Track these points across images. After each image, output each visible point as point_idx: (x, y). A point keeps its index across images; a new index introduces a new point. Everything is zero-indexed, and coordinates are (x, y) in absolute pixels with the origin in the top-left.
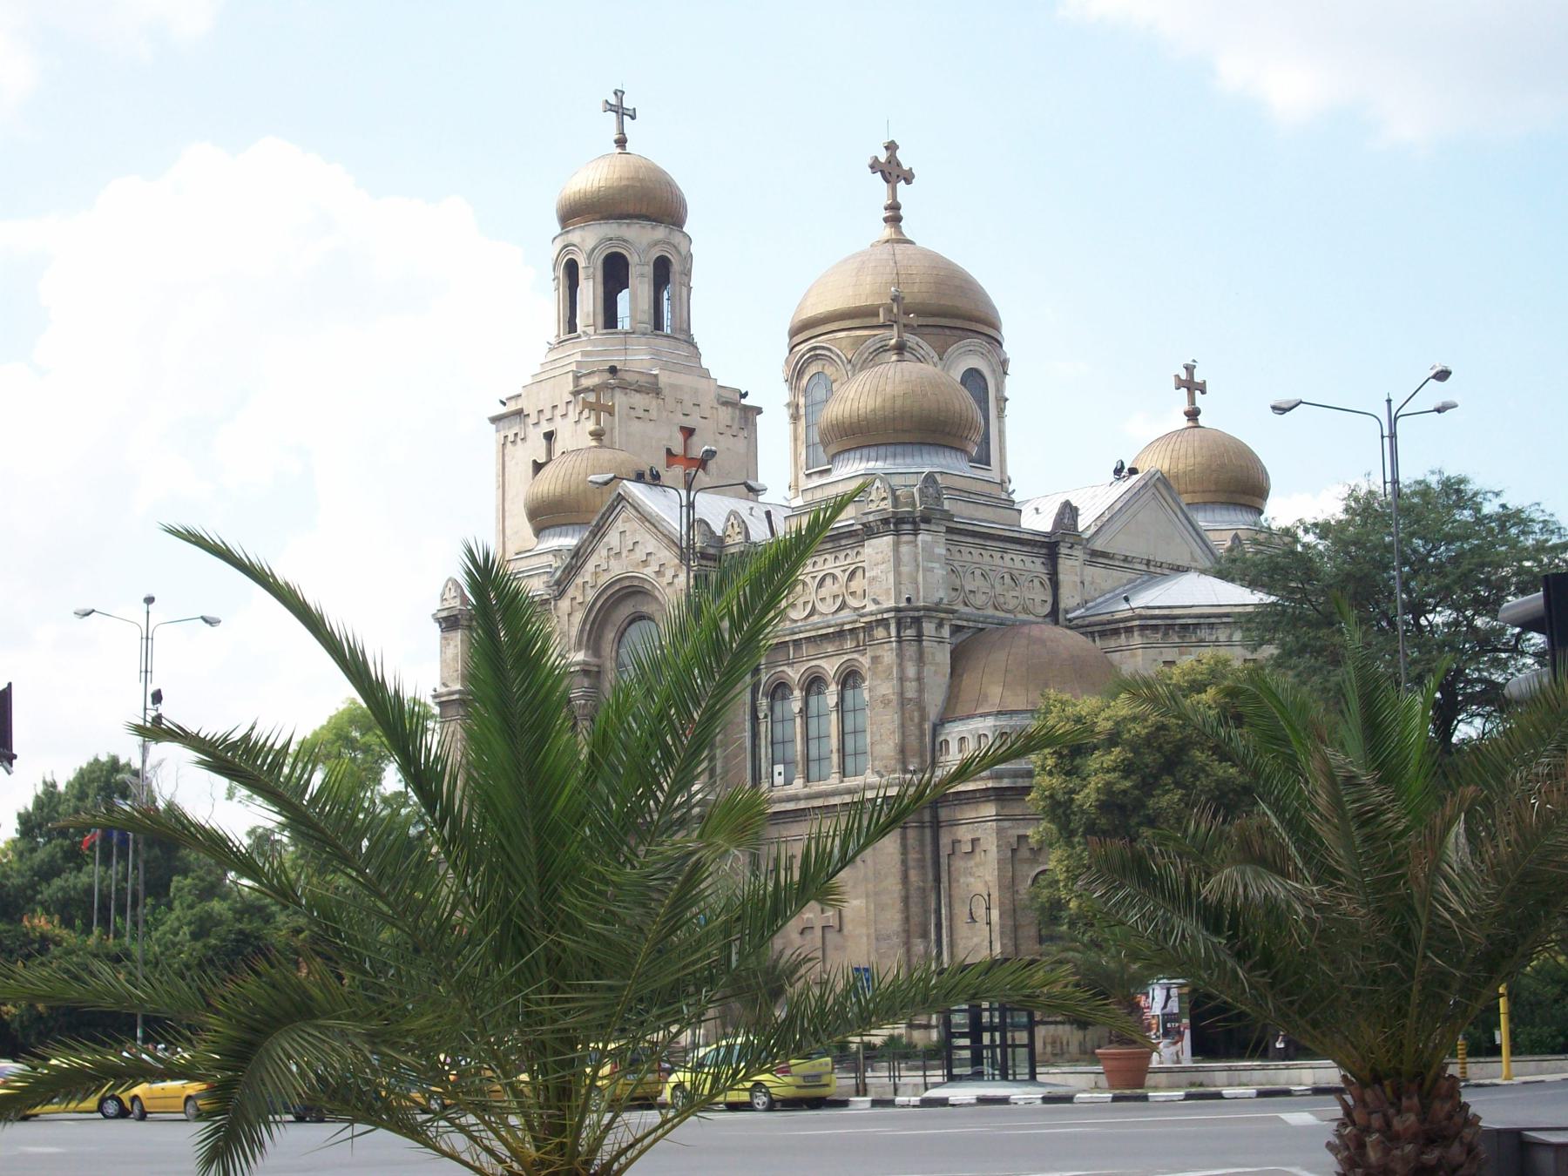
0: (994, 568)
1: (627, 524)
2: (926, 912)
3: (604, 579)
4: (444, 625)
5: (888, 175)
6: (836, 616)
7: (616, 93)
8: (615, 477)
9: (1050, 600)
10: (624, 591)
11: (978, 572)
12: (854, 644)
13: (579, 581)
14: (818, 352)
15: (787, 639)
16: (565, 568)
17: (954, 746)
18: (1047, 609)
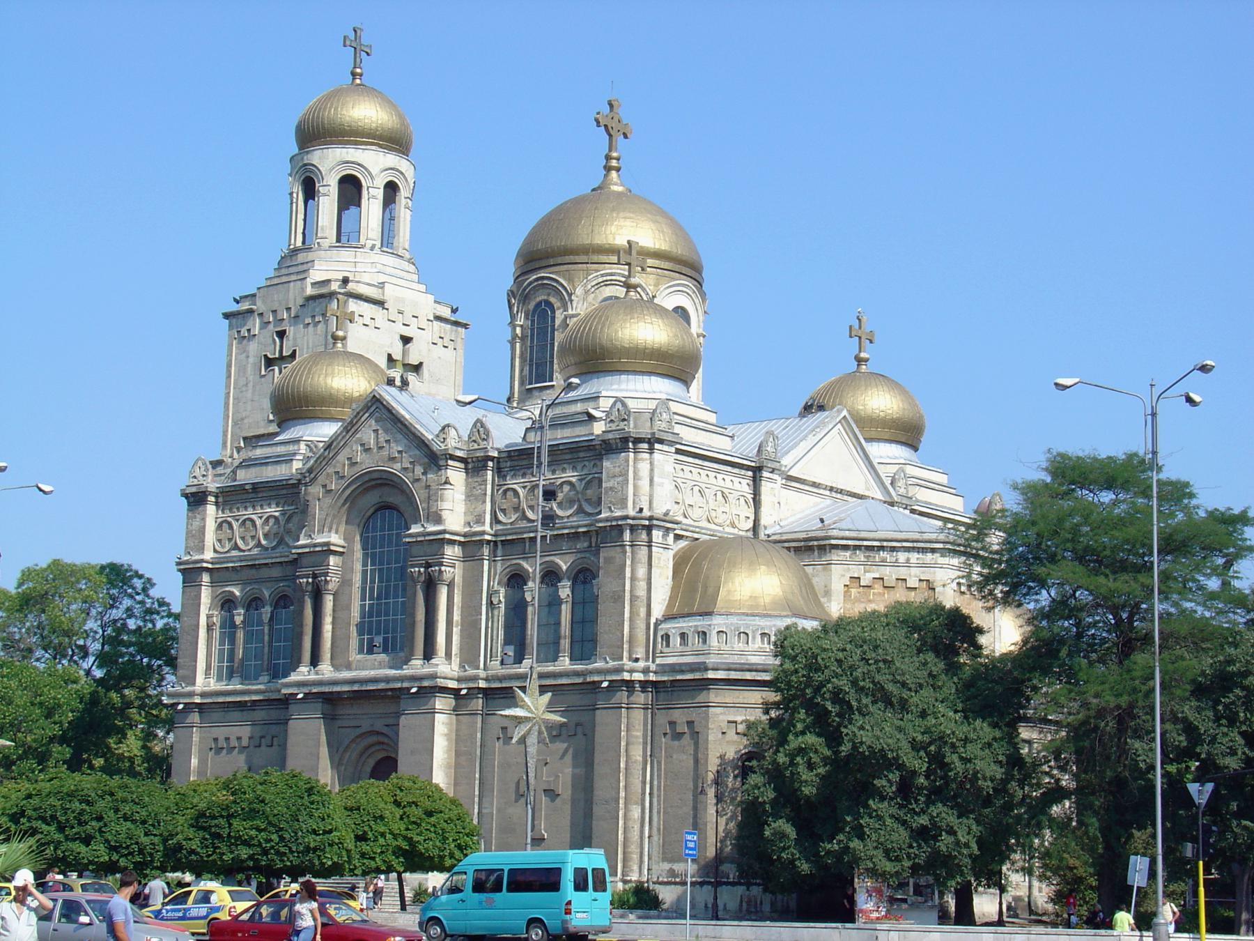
0: (708, 486)
2: (644, 782)
4: (192, 500)
5: (610, 129)
6: (571, 520)
7: (355, 31)
8: (478, 399)
9: (752, 518)
10: (373, 483)
11: (696, 489)
12: (586, 544)
13: (330, 470)
14: (545, 282)
15: (525, 536)
16: (318, 458)
17: (676, 641)
18: (750, 524)
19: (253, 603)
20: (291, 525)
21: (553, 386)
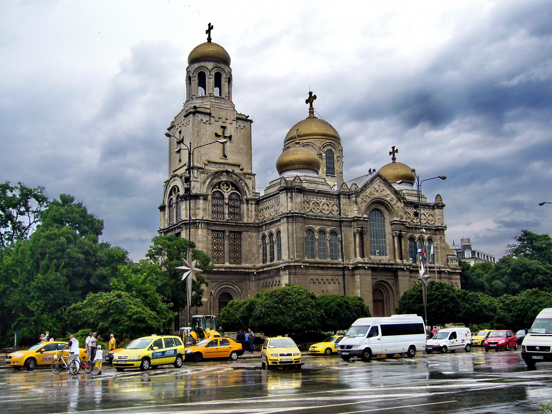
1: (380, 184)
3: (373, 196)
12: (430, 232)
19: (322, 232)
20: (333, 208)
21: (335, 176)
